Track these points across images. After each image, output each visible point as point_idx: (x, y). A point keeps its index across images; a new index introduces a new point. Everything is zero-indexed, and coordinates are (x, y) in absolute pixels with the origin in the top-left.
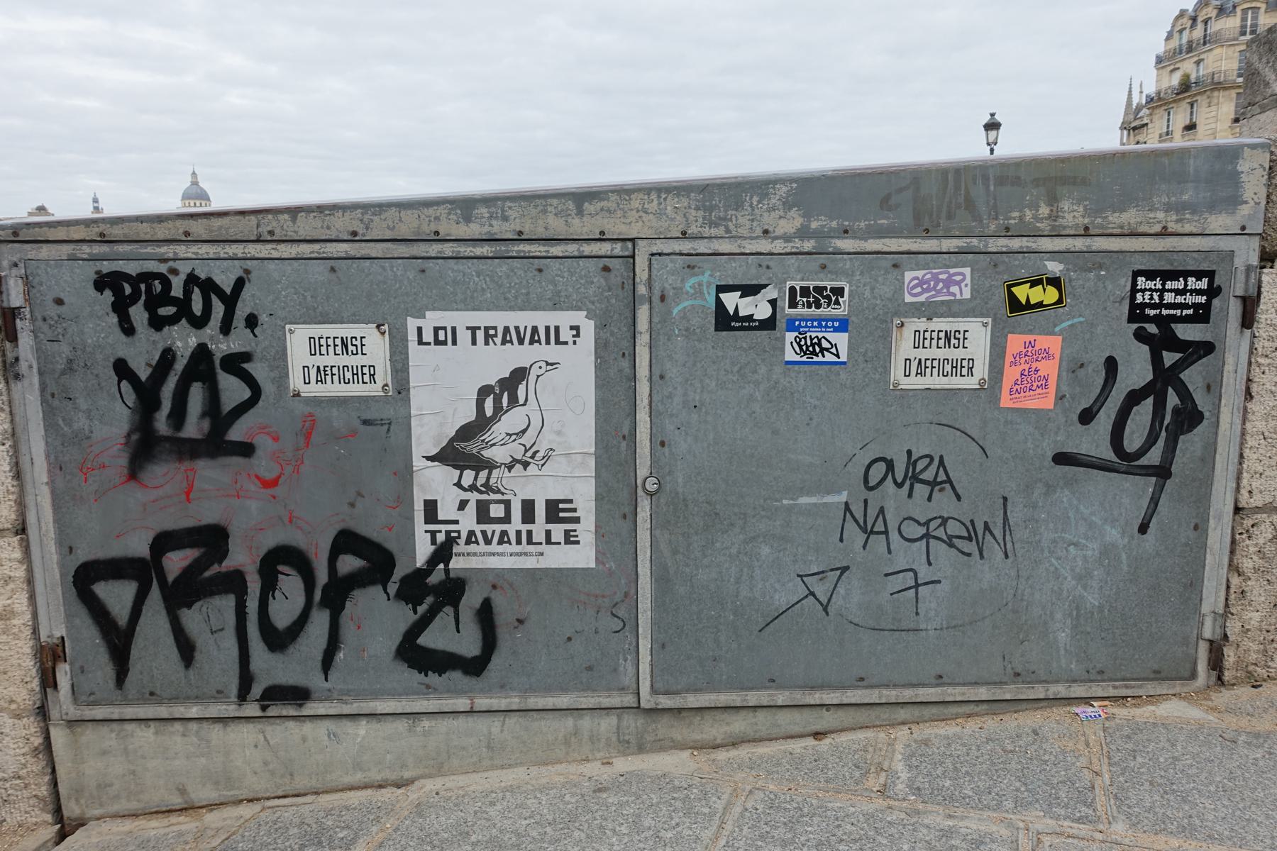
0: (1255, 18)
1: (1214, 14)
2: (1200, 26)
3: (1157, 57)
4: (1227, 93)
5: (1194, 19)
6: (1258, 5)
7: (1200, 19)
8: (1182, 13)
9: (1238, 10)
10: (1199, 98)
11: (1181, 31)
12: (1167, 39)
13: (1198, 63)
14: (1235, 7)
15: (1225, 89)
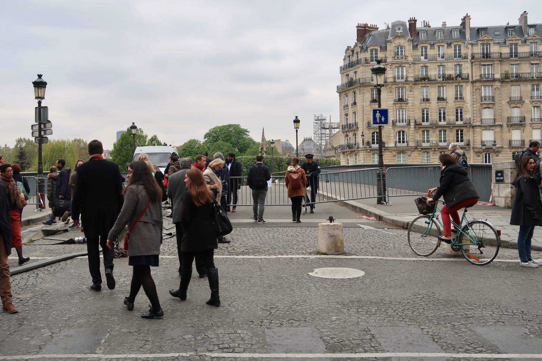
0: (376, 54)
1: (359, 50)
2: (355, 55)
3: (341, 68)
4: (367, 88)
5: (353, 51)
6: (377, 48)
7: (355, 52)
8: (348, 48)
9: (369, 49)
10: (356, 90)
11: (349, 57)
12: (344, 60)
13: (356, 72)
14: (367, 48)
15: (365, 86)
